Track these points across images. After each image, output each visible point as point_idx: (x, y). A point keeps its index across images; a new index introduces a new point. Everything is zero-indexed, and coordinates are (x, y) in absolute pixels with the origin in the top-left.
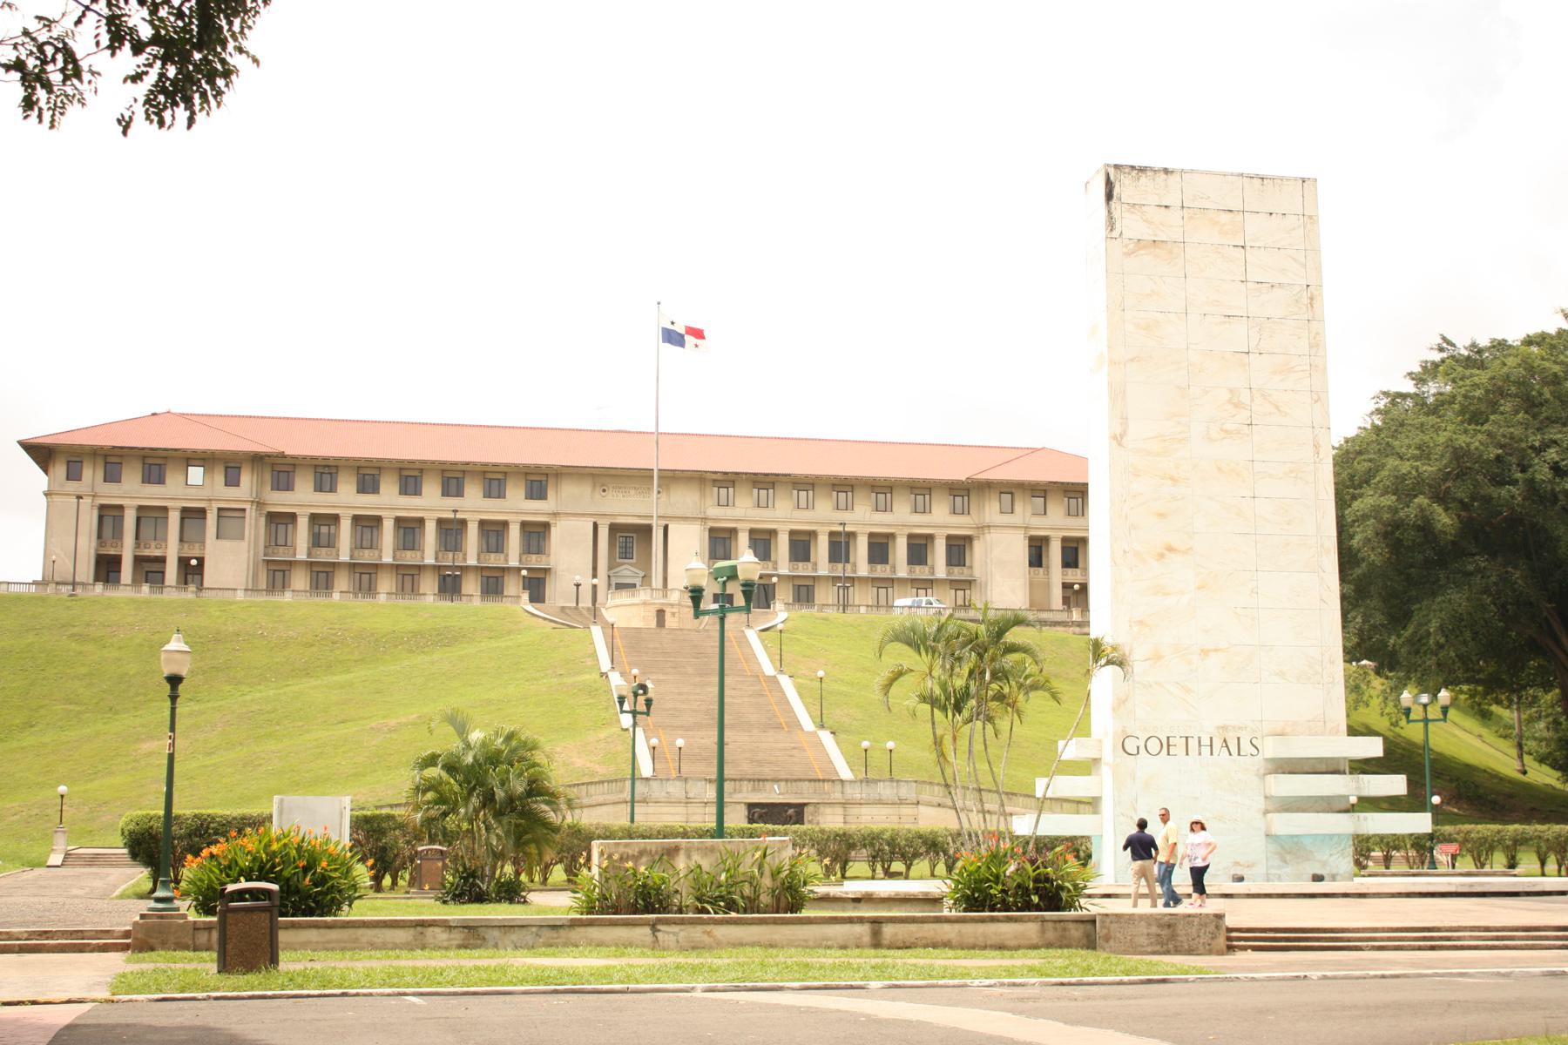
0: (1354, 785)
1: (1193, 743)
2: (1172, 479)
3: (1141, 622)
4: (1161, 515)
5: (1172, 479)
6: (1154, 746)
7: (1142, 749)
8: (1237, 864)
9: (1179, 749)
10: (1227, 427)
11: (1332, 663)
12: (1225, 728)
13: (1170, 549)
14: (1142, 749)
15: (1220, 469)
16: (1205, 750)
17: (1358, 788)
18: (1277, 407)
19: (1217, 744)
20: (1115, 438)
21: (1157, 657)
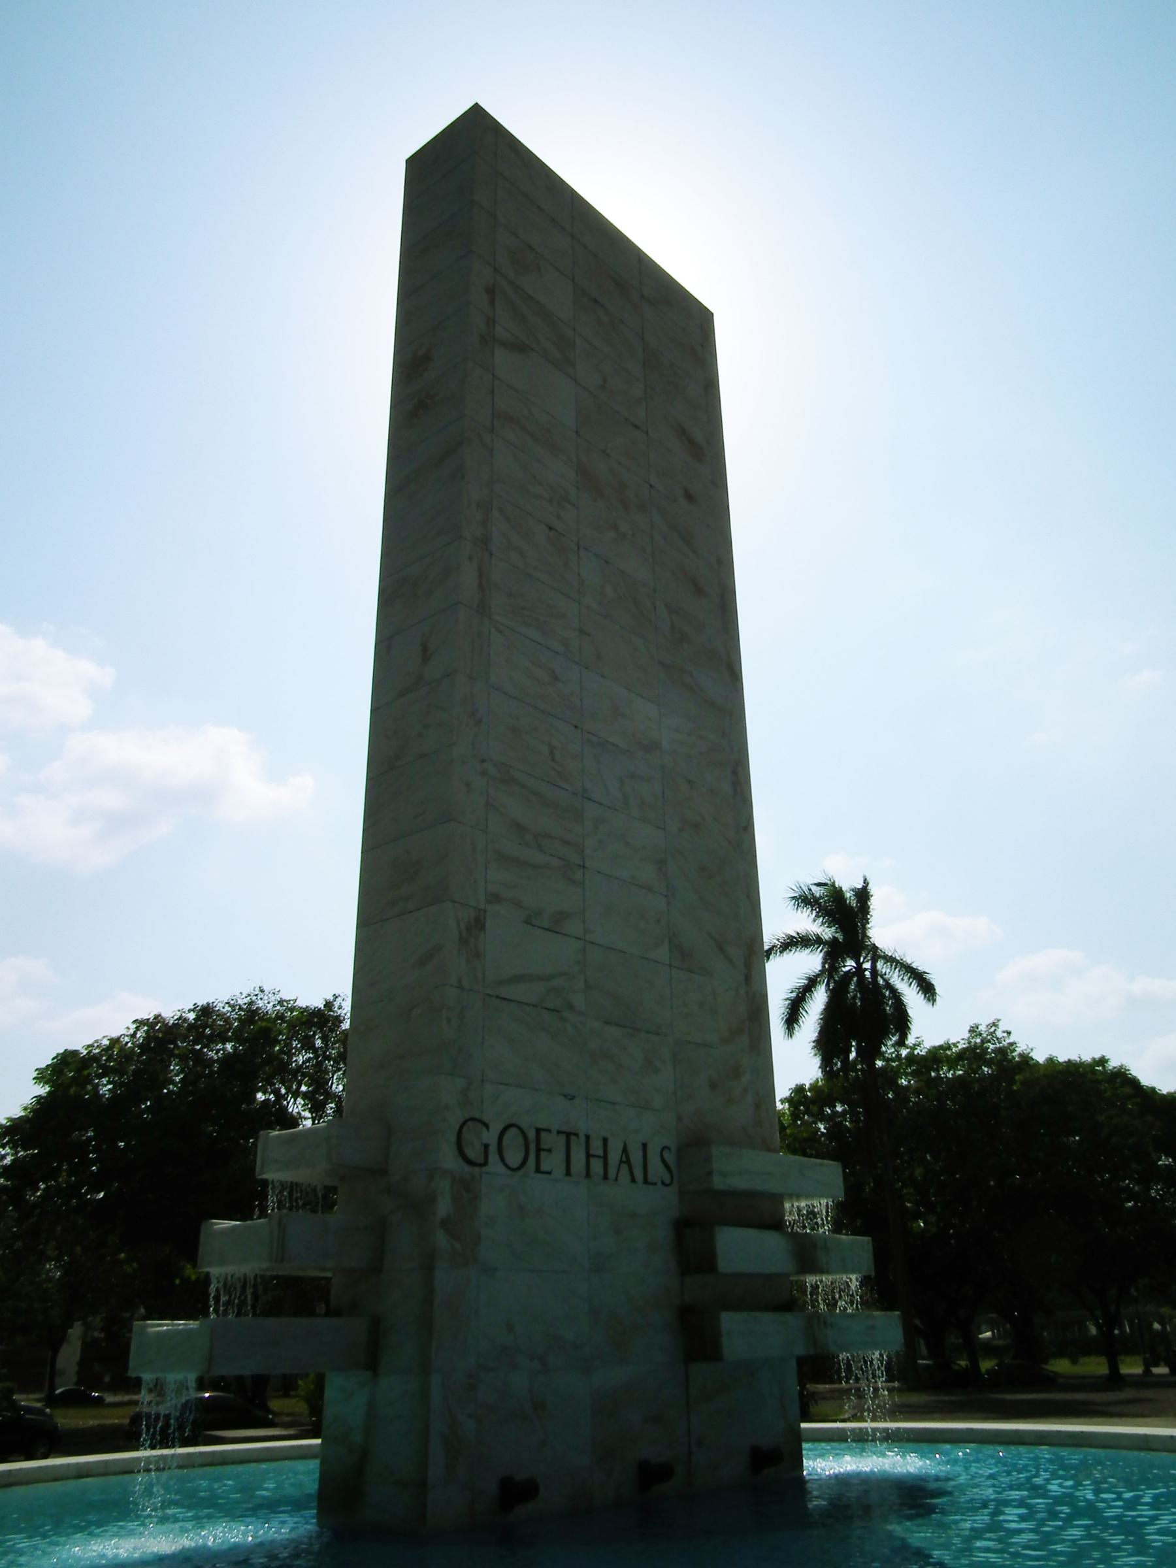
7: (493, 1157)
9: (553, 1162)
14: (493, 1157)
16: (597, 1166)
19: (614, 1156)
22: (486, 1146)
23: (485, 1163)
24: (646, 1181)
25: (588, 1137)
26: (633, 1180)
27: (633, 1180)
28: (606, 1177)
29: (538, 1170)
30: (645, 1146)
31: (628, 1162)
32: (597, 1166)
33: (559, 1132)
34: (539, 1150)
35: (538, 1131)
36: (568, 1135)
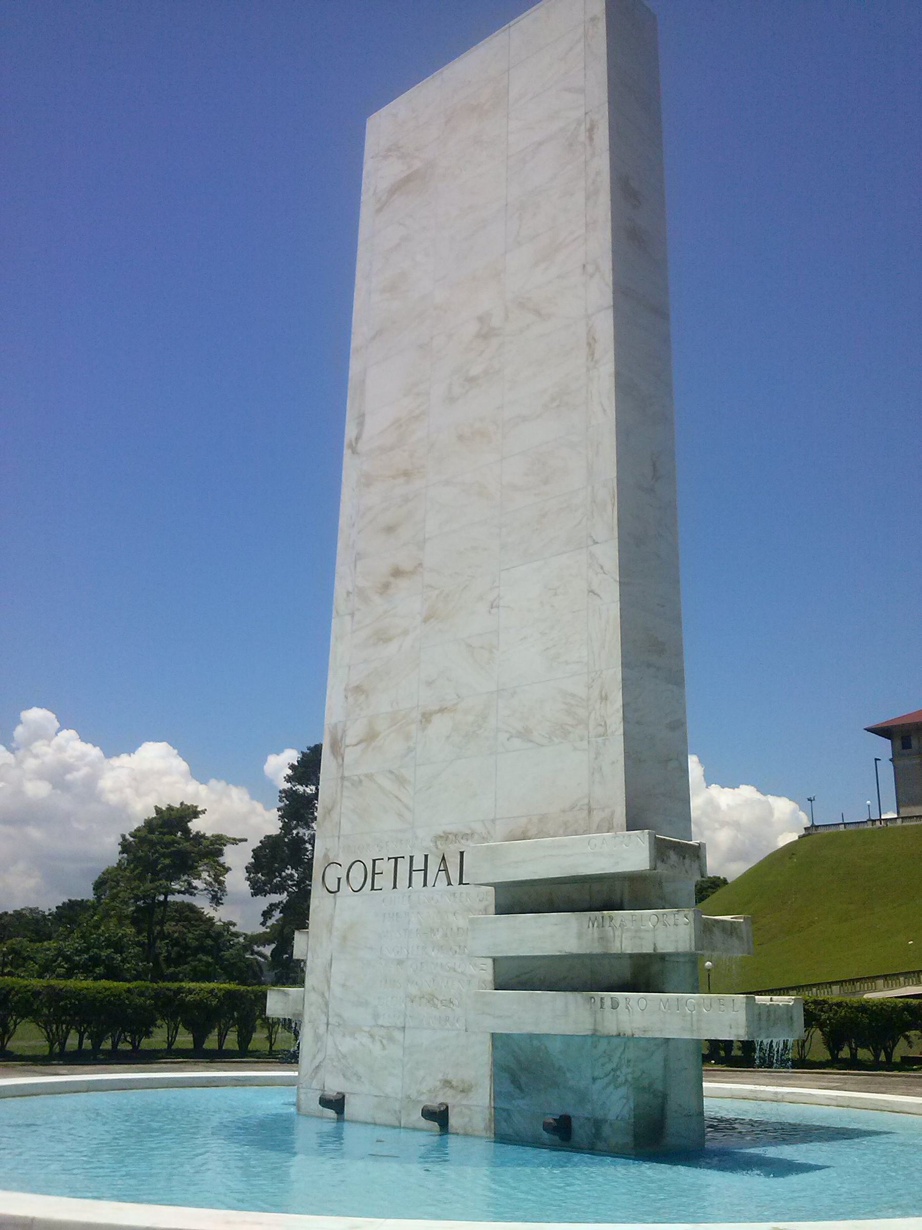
0: (595, 932)
1: (403, 866)
2: (406, 474)
3: (358, 689)
4: (390, 529)
5: (406, 474)
6: (357, 874)
8: (447, 1083)
10: (475, 371)
11: (604, 698)
12: (445, 837)
13: (397, 573)
15: (461, 438)
16: (418, 877)
17: (602, 939)
18: (538, 313)
20: (351, 446)
21: (371, 737)
22: (339, 879)
23: (339, 890)
24: (461, 883)
25: (411, 857)
26: (449, 884)
27: (449, 884)
28: (425, 885)
29: (373, 889)
30: (462, 853)
31: (446, 870)
32: (418, 877)
33: (389, 859)
34: (374, 873)
35: (374, 861)
36: (396, 859)
